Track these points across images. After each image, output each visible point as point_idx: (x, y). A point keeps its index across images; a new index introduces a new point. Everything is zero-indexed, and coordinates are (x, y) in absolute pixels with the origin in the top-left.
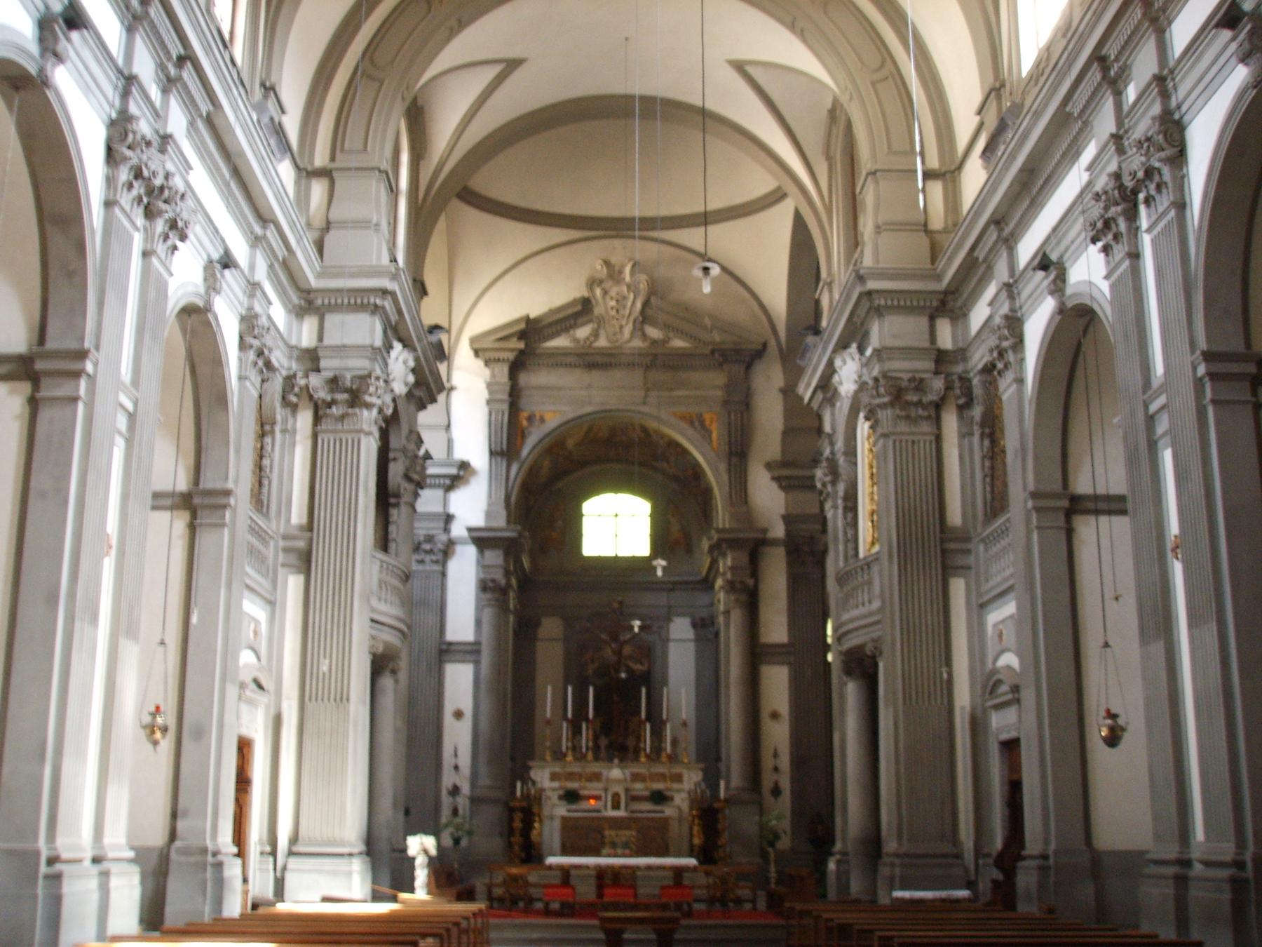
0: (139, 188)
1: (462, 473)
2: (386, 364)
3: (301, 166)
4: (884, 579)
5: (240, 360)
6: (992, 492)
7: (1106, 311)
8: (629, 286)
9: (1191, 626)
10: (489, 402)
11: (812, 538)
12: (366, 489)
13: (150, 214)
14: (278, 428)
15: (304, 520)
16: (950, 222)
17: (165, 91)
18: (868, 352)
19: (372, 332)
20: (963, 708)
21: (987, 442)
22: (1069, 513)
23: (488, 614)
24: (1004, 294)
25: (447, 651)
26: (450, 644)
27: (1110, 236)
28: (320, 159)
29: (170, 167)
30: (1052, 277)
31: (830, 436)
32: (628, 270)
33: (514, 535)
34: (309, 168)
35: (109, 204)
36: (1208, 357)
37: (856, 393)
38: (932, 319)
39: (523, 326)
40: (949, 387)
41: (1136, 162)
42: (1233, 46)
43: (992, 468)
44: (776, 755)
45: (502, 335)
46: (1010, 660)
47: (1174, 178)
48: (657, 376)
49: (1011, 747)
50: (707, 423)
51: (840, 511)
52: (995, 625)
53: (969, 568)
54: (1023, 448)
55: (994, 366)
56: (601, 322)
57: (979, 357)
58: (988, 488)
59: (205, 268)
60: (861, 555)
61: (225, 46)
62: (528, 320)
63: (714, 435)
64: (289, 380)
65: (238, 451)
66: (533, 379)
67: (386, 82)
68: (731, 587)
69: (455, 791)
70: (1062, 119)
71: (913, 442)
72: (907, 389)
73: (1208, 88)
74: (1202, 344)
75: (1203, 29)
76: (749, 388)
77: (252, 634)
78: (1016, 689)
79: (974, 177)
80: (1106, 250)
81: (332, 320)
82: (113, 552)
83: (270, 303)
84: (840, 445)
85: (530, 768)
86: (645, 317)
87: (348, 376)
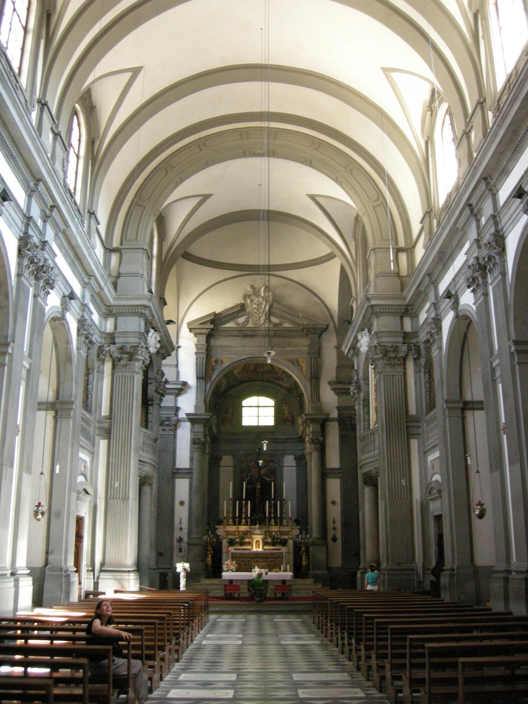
0: (32, 268)
1: (183, 388)
2: (146, 340)
3: (107, 247)
4: (380, 439)
5: (78, 340)
6: (430, 399)
7: (475, 317)
8: (263, 298)
9: (509, 466)
10: (196, 353)
11: (351, 417)
12: (137, 399)
13: (37, 278)
14: (95, 370)
15: (108, 414)
16: (410, 272)
17: (45, 221)
18: (373, 333)
19: (140, 325)
20: (417, 500)
21: (427, 376)
22: (463, 410)
23: (196, 455)
24: (433, 308)
25: (176, 473)
26: (178, 469)
27: (475, 286)
28: (116, 244)
29: (47, 256)
30: (452, 301)
31: (357, 371)
32: (262, 290)
33: (209, 417)
34: (110, 248)
35: (19, 275)
36: (516, 343)
37: (368, 351)
38: (402, 318)
39: (212, 317)
40: (409, 350)
41: (485, 253)
42: (522, 205)
43: (430, 388)
44: (334, 522)
45: (202, 321)
46: (437, 477)
47: (501, 261)
48: (276, 341)
49: (438, 518)
50: (300, 363)
51: (362, 406)
52: (431, 461)
53: (420, 434)
54: (442, 379)
55: (429, 341)
56: (250, 315)
57: (423, 336)
58: (428, 397)
59: (62, 299)
60: (371, 428)
61: (72, 197)
62: (215, 314)
63: (304, 369)
64: (101, 349)
65: (77, 383)
66: (219, 342)
67: (146, 208)
68: (312, 441)
69: (180, 540)
70: (454, 231)
71: (393, 376)
72: (390, 351)
73: (514, 223)
74: (513, 337)
75: (510, 196)
76: (320, 346)
77: (83, 468)
78: (440, 491)
79: (420, 252)
80: (473, 291)
81: (121, 319)
82: (20, 433)
83: (92, 314)
84: (361, 375)
85: (217, 529)
86: (270, 313)
87: (129, 346)
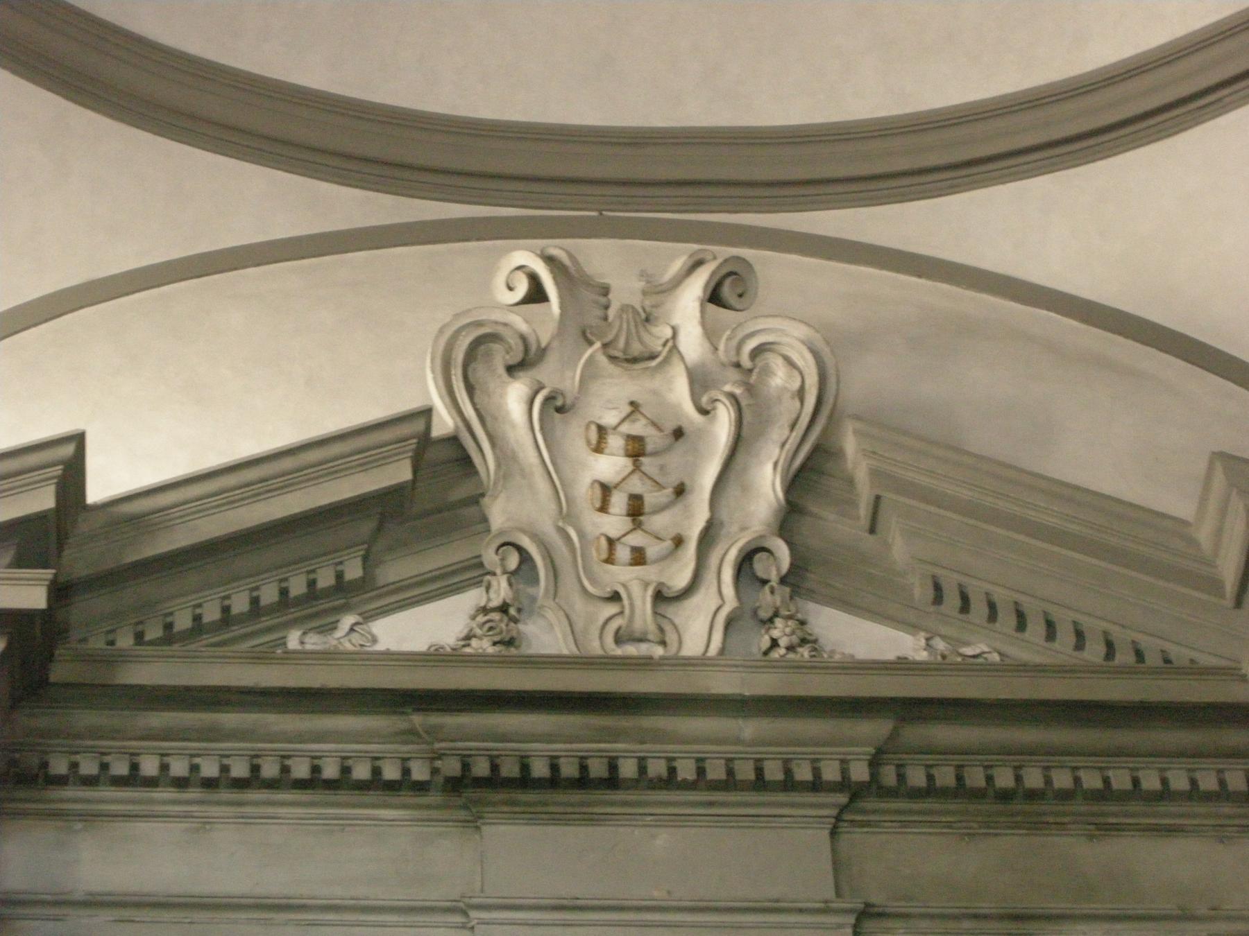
8: (699, 381)
39: (44, 500)
86: (801, 559)
